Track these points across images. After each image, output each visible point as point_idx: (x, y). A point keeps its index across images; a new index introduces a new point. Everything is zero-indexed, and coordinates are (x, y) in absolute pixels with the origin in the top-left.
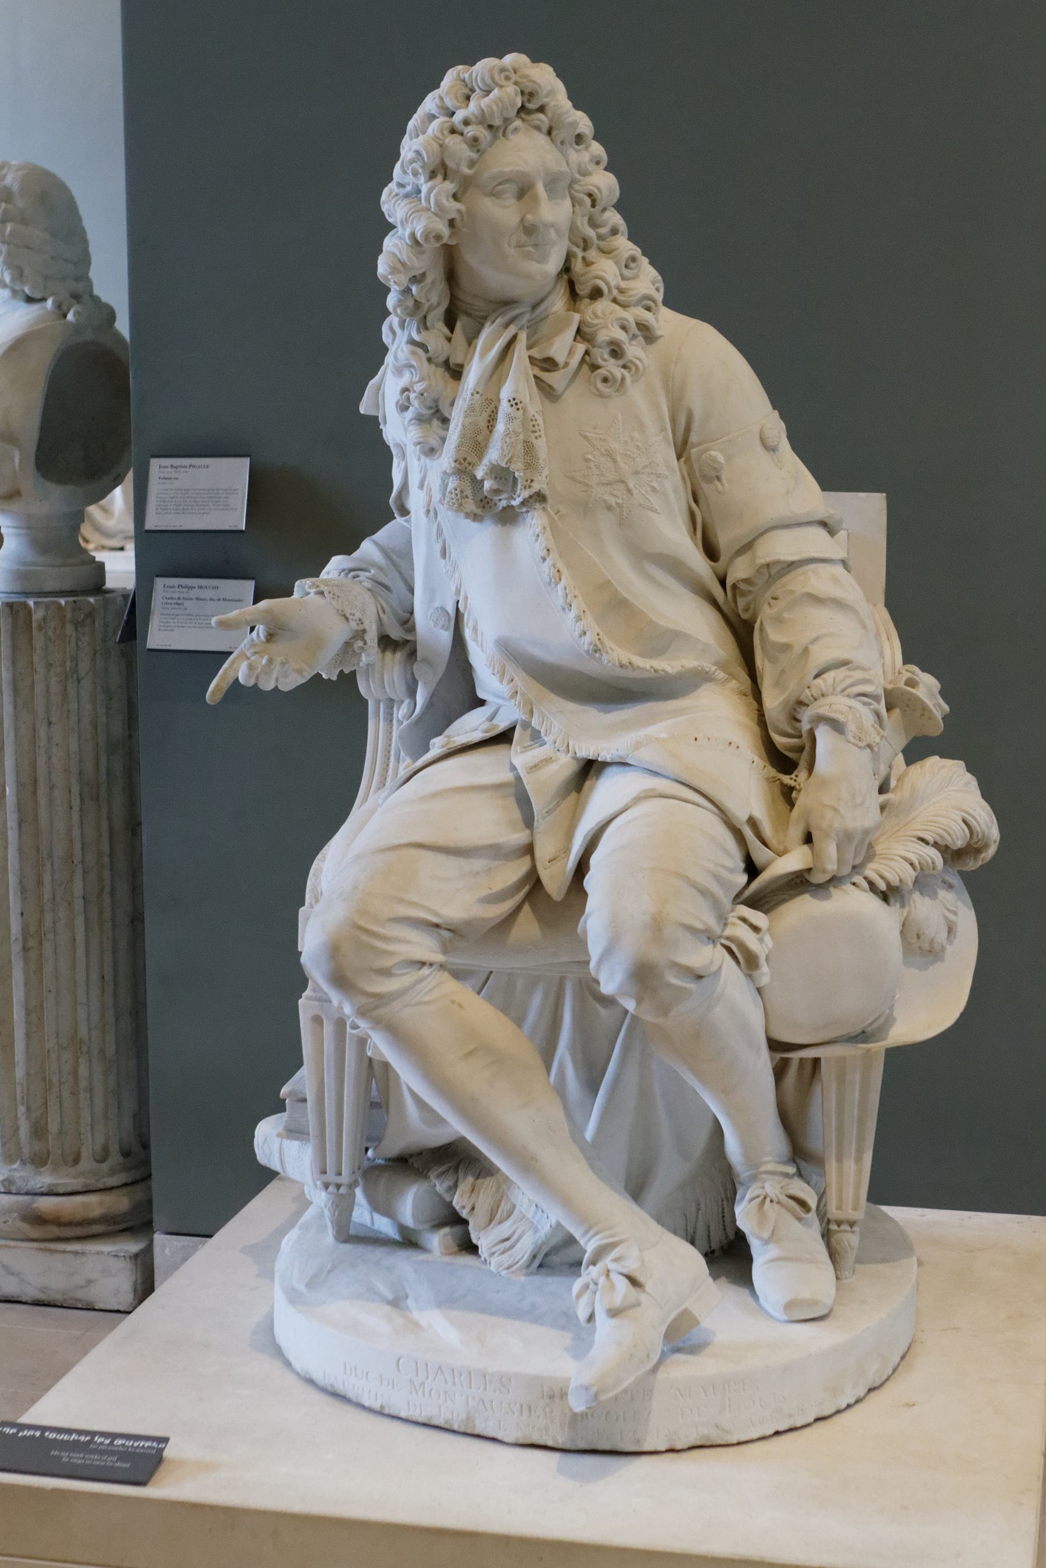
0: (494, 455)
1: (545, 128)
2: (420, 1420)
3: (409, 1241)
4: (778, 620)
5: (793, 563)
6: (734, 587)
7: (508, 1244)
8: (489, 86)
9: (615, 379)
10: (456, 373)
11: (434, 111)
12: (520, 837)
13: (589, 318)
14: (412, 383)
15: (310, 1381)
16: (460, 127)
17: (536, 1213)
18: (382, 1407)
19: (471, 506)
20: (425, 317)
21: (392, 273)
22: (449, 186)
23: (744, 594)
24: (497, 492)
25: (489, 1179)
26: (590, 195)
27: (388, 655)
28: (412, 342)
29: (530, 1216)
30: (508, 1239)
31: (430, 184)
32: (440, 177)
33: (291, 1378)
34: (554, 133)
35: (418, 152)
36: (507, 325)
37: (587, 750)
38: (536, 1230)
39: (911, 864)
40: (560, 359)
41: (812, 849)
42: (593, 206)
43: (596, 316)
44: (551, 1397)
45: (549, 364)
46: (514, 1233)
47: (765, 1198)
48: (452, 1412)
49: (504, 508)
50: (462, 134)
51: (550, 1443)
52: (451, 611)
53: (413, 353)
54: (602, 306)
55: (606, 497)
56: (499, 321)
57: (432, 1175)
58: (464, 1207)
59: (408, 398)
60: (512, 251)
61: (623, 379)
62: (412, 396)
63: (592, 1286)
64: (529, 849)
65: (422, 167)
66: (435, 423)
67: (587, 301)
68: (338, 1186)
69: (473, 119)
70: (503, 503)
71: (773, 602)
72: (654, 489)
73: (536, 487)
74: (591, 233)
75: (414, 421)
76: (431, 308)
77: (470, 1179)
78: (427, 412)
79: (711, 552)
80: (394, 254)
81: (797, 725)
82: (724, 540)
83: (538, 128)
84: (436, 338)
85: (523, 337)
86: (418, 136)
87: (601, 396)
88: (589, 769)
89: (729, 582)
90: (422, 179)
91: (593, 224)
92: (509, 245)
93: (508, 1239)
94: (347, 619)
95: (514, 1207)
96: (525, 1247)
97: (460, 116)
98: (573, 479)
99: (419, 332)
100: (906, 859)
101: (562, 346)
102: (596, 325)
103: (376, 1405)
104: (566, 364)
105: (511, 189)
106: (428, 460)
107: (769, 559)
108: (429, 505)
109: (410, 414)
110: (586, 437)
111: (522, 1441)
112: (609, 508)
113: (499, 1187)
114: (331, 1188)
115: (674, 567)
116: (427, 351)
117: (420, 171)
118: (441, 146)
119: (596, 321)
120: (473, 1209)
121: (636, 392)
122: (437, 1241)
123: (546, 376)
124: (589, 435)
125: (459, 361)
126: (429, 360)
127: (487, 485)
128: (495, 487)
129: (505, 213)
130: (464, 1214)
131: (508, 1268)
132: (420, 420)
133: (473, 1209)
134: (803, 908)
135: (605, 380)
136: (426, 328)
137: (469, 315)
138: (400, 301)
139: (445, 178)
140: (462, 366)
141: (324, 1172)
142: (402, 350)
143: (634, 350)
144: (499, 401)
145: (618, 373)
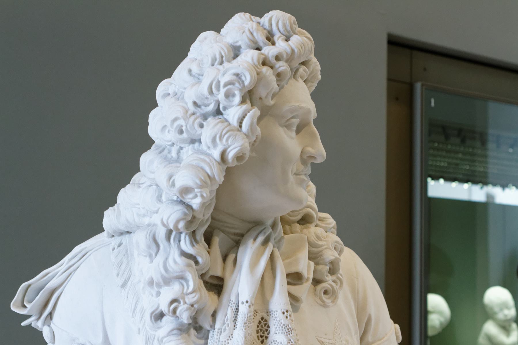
8: (288, 32)
10: (216, 286)
11: (242, 41)
14: (184, 295)
16: (273, 61)
20: (194, 232)
21: (201, 187)
22: (255, 112)
28: (184, 254)
31: (244, 107)
35: (237, 75)
36: (266, 242)
40: (305, 274)
45: (294, 278)
50: (272, 67)
53: (189, 265)
54: (313, 230)
56: (261, 239)
60: (291, 177)
65: (241, 90)
66: (193, 332)
67: (298, 225)
69: (285, 56)
75: (175, 332)
76: (201, 225)
80: (202, 169)
84: (200, 251)
85: (277, 253)
86: (221, 63)
87: (324, 305)
90: (237, 99)
92: (292, 172)
97: (269, 51)
102: (322, 246)
105: (296, 121)
116: (197, 262)
117: (237, 93)
118: (258, 74)
119: (320, 243)
123: (294, 289)
124: (324, 340)
125: (219, 274)
135: (326, 292)
136: (197, 242)
137: (223, 232)
138: (185, 214)
139: (252, 105)
140: (221, 280)
142: (175, 262)
144: (268, 313)
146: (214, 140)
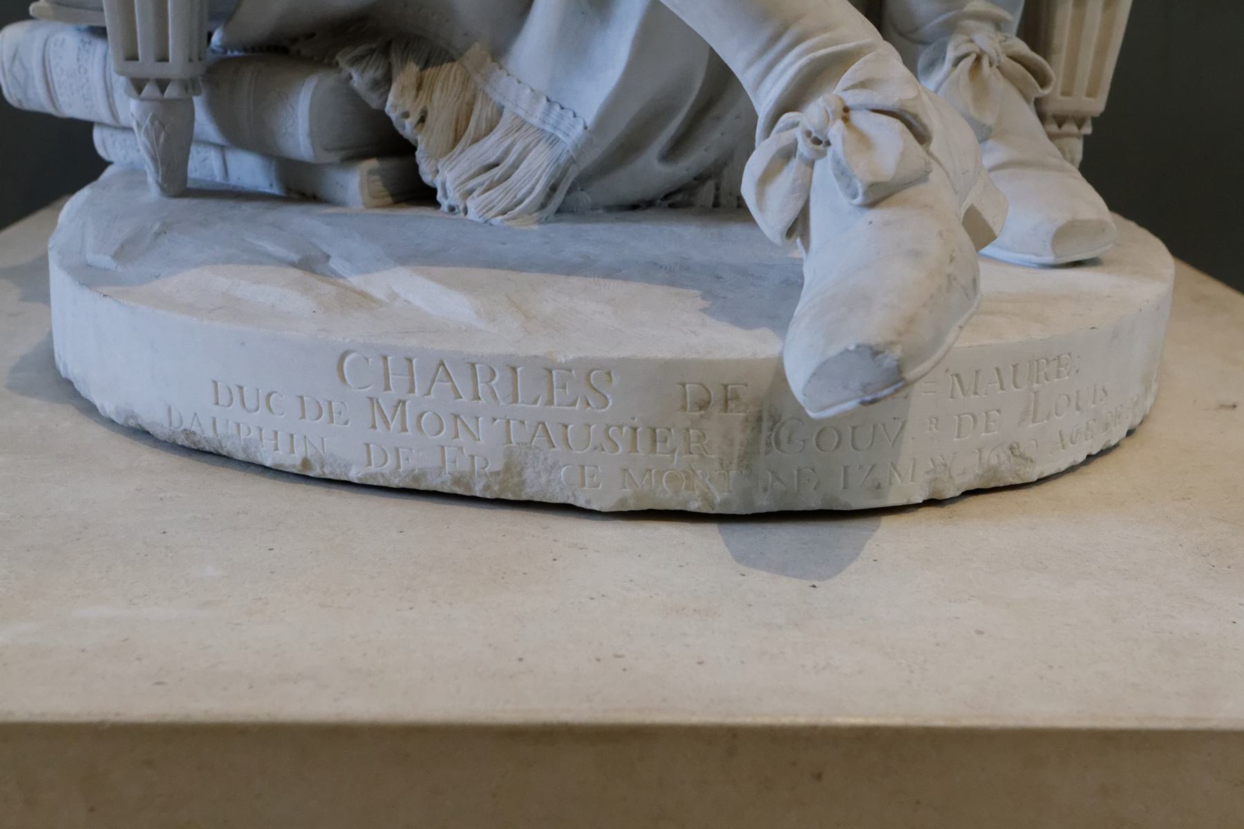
2: (395, 482)
3: (300, 187)
7: (497, 172)
15: (141, 434)
17: (548, 112)
18: (306, 463)
25: (446, 66)
29: (535, 120)
30: (495, 165)
33: (100, 432)
38: (553, 141)
44: (703, 405)
46: (506, 153)
47: (978, 59)
48: (474, 455)
51: (694, 506)
57: (342, 59)
58: (406, 115)
63: (804, 148)
68: (162, 84)
77: (413, 69)
93: (495, 165)
95: (500, 111)
96: (536, 170)
103: (292, 461)
111: (632, 506)
113: (467, 80)
114: (149, 90)
120: (422, 120)
122: (356, 183)
130: (407, 128)
131: (504, 213)
133: (422, 120)
141: (133, 57)
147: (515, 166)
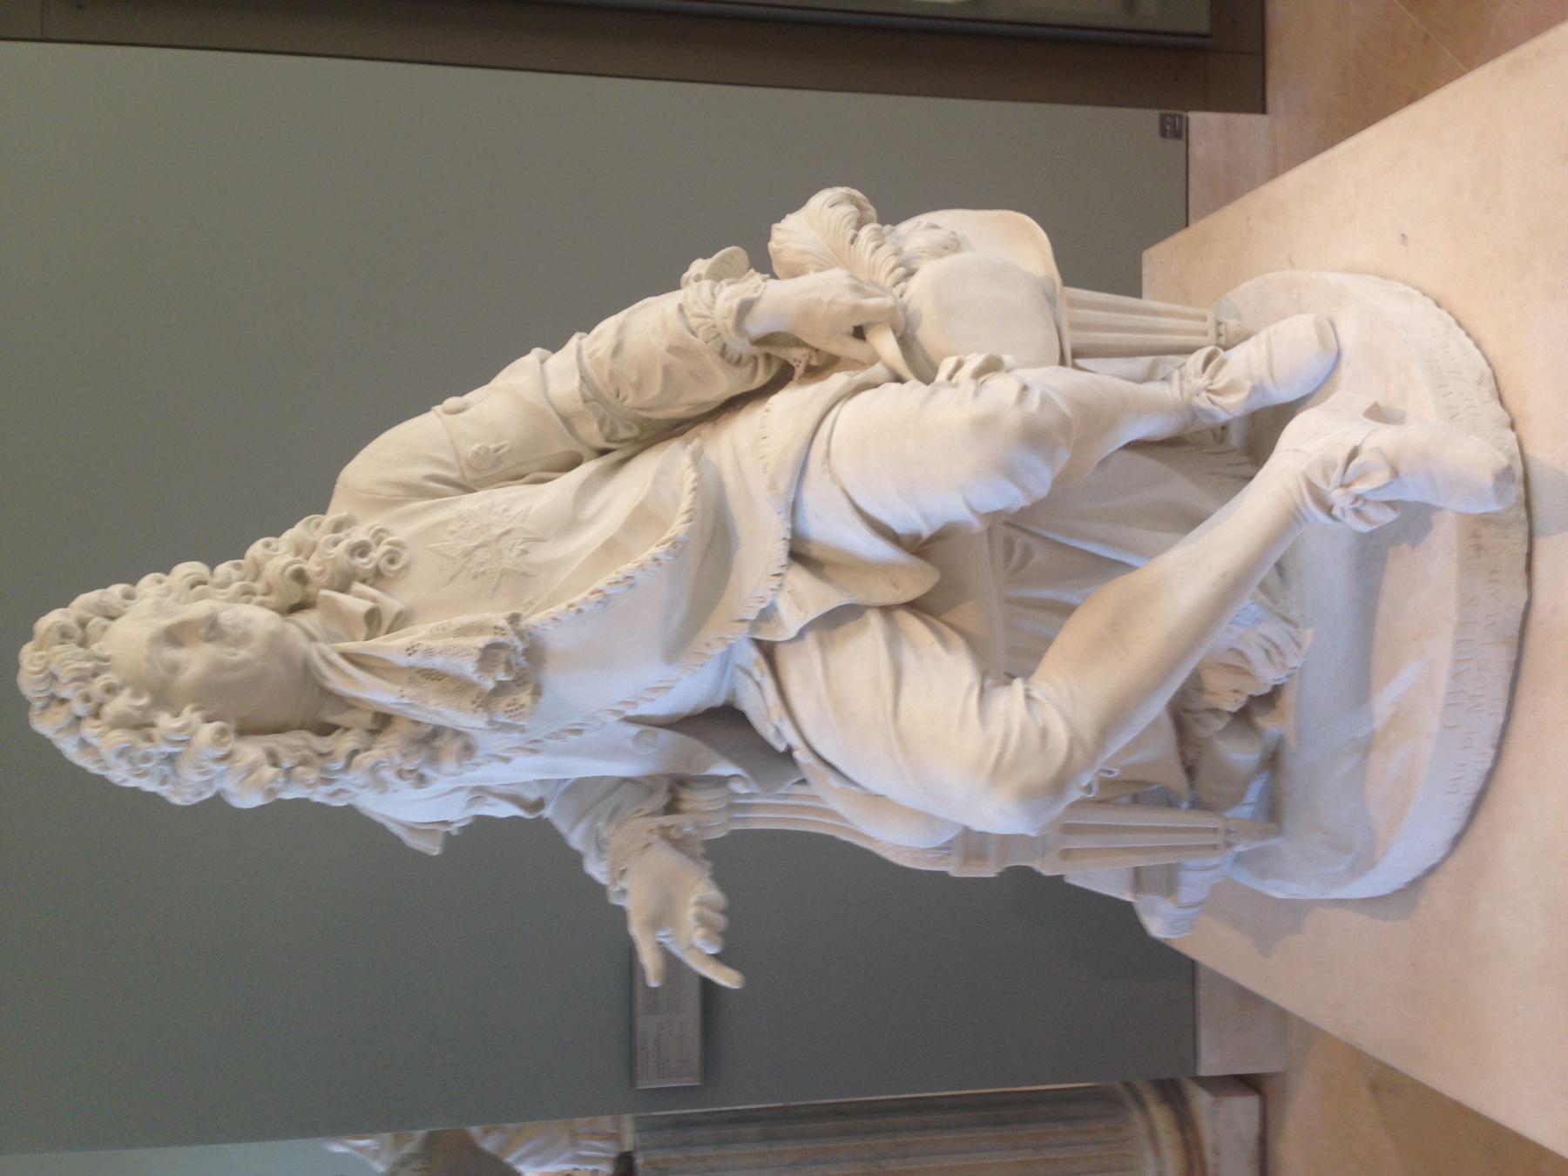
0: (469, 668)
1: (105, 622)
3: (1273, 760)
4: (639, 387)
5: (582, 378)
6: (608, 440)
7: (1273, 650)
9: (389, 552)
10: (383, 721)
11: (74, 740)
12: (874, 620)
13: (324, 580)
19: (524, 697)
23: (614, 430)
24: (509, 667)
26: (193, 586)
27: (685, 806)
32: (154, 731)
34: (113, 613)
37: (779, 551)
39: (878, 247)
41: (872, 324)
42: (205, 583)
43: (321, 573)
48: (1498, 660)
49: (528, 660)
50: (101, 705)
51: (1525, 549)
52: (634, 730)
55: (513, 554)
59: (411, 771)
61: (390, 543)
62: (408, 767)
63: (1357, 505)
64: (886, 610)
66: (438, 743)
70: (521, 659)
71: (622, 396)
72: (505, 510)
73: (503, 623)
74: (236, 586)
77: (1207, 697)
78: (424, 754)
79: (573, 463)
81: (745, 358)
82: (561, 446)
83: (105, 628)
87: (406, 567)
88: (800, 554)
89: (602, 444)
91: (225, 584)
93: (1267, 652)
94: (648, 845)
95: (1231, 650)
97: (79, 708)
98: (495, 589)
99: (334, 760)
100: (873, 252)
101: (356, 602)
103: (1491, 752)
104: (374, 600)
106: (480, 753)
107: (578, 397)
108: (525, 749)
109: (428, 772)
110: (452, 579)
112: (525, 552)
115: (586, 490)
116: (355, 752)
120: (1236, 691)
121: (400, 533)
122: (1270, 725)
123: (386, 623)
126: (368, 749)
127: (502, 676)
128: (502, 667)
129: (195, 660)
130: (1243, 699)
132: (433, 760)
133: (1236, 691)
134: (928, 335)
139: (153, 725)
141: (1215, 847)
143: (359, 534)
144: (411, 668)
145: (384, 548)
146: (205, 773)
147: (1269, 640)
